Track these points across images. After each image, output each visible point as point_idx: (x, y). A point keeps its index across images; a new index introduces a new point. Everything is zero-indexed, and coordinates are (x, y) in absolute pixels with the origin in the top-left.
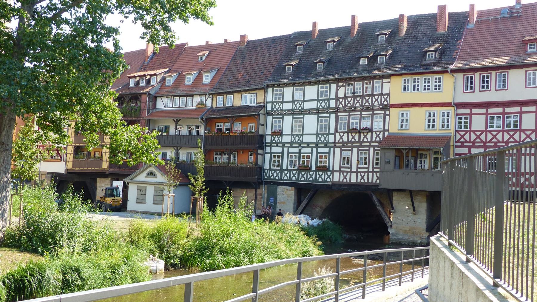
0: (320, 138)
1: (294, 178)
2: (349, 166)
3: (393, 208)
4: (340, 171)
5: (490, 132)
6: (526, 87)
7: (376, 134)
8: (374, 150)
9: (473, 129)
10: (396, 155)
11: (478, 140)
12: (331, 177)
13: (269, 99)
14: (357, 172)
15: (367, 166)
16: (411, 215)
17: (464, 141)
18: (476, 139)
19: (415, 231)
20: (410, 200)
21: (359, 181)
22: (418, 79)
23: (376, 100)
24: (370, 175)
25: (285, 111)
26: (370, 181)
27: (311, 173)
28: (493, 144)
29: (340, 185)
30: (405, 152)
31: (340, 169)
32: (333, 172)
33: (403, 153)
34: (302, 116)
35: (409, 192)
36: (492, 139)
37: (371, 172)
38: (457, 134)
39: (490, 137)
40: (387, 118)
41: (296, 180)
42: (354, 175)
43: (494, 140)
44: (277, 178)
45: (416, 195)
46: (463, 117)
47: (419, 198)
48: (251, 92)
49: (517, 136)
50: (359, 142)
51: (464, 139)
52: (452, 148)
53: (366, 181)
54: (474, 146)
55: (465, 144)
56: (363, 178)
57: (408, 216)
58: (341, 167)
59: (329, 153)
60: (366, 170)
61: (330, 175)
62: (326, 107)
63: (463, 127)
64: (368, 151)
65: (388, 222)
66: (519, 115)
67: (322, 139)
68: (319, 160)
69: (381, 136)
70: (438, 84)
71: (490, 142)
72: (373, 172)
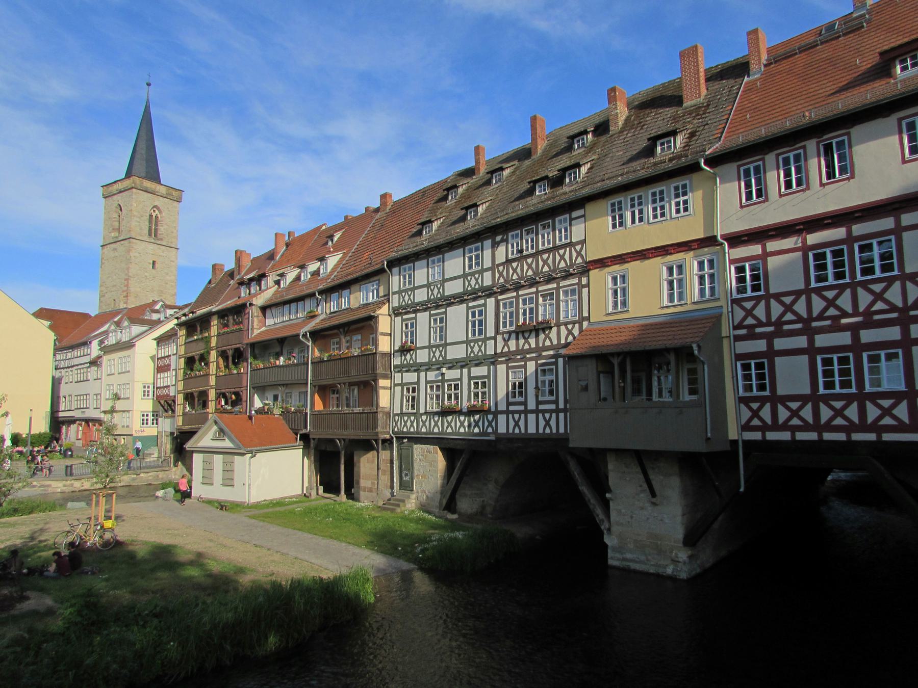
0: (472, 348)
1: (436, 430)
2: (522, 399)
3: (609, 491)
4: (507, 412)
5: (818, 291)
6: (904, 161)
7: (567, 329)
9: (772, 291)
10: (600, 369)
11: (789, 316)
12: (493, 424)
13: (395, 287)
14: (537, 411)
15: (553, 398)
16: (647, 505)
19: (659, 542)
20: (639, 469)
21: (541, 431)
22: (640, 197)
23: (562, 257)
24: (562, 415)
25: (418, 304)
28: (828, 323)
29: (508, 439)
30: (616, 361)
31: (507, 407)
32: (496, 413)
33: (613, 365)
34: (444, 310)
36: (825, 309)
37: (561, 411)
38: (736, 308)
40: (585, 290)
41: (439, 433)
42: (532, 417)
43: (832, 312)
44: (412, 430)
48: (371, 280)
49: (894, 295)
52: (725, 343)
53: (554, 431)
54: (780, 333)
55: (758, 330)
56: (547, 423)
57: (642, 508)
58: (509, 404)
59: (488, 377)
60: (553, 407)
61: (492, 421)
62: (477, 287)
63: (749, 289)
64: (554, 367)
65: (603, 521)
66: (893, 237)
67: (476, 349)
69: (576, 332)
70: (682, 199)
71: (821, 317)
72: (565, 411)
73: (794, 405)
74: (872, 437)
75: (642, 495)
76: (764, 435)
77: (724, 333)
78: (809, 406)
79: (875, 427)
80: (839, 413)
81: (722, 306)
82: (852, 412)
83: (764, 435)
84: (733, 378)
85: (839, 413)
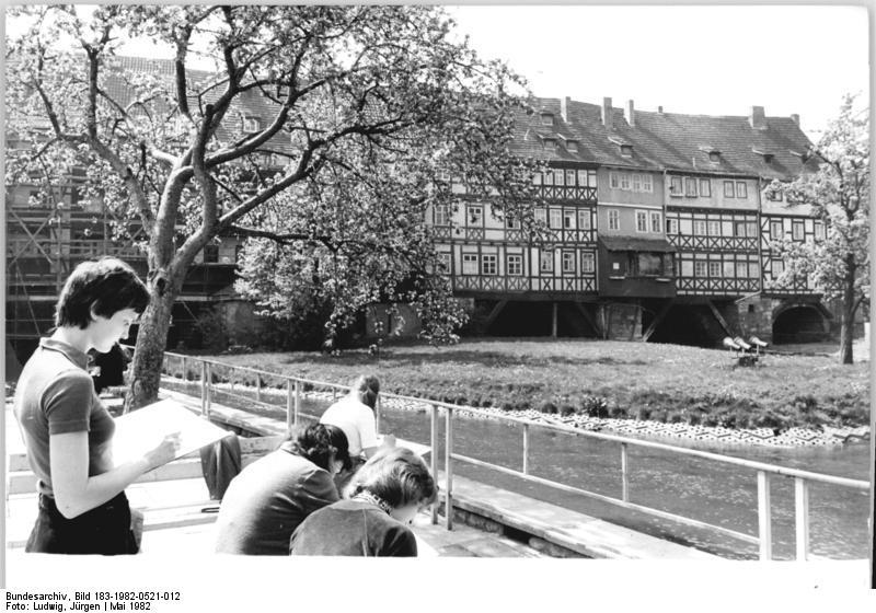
4: (539, 278)
8: (581, 252)
12: (528, 284)
14: (562, 278)
23: (582, 194)
24: (579, 281)
26: (579, 289)
27: (499, 280)
32: (530, 277)
40: (594, 215)
42: (558, 282)
50: (563, 241)
58: (540, 272)
59: (523, 254)
60: (573, 276)
68: (509, 263)
69: (589, 235)
72: (582, 278)
74: (710, 293)
82: (706, 284)
85: (702, 284)
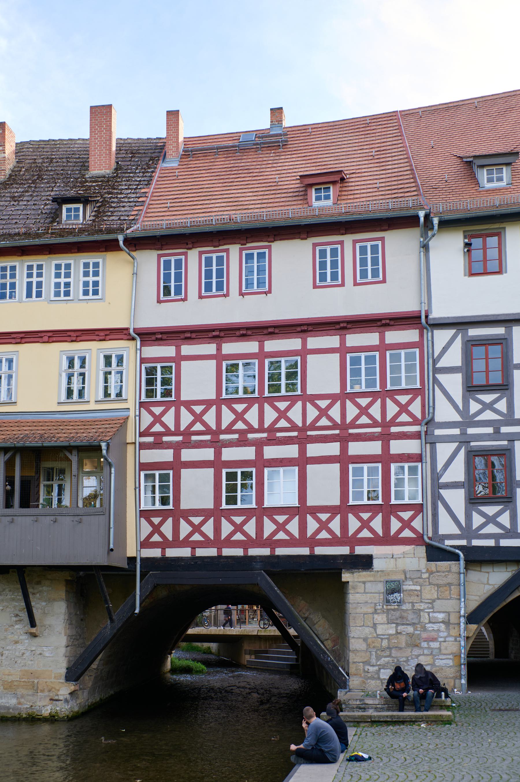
9: (183, 398)
11: (198, 427)
16: (24, 637)
17: (163, 430)
18: (192, 424)
19: (36, 681)
20: (20, 596)
22: (40, 267)
35: (15, 576)
39: (227, 417)
45: (39, 583)
46: (159, 366)
47: (45, 588)
51: (163, 425)
52: (130, 449)
54: (188, 444)
55: (165, 439)
57: (16, 642)
71: (229, 430)
73: (196, 520)
74: (266, 552)
75: (17, 627)
76: (163, 552)
77: (130, 438)
78: (211, 522)
79: (271, 543)
80: (239, 528)
81: (129, 409)
82: (251, 528)
83: (163, 552)
84: (135, 489)
85: (239, 528)
